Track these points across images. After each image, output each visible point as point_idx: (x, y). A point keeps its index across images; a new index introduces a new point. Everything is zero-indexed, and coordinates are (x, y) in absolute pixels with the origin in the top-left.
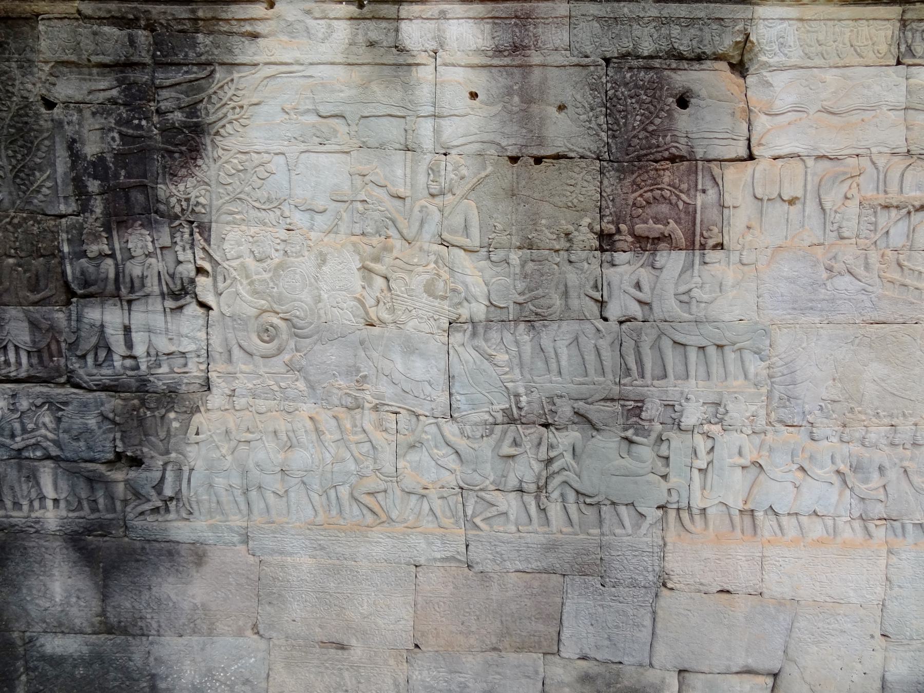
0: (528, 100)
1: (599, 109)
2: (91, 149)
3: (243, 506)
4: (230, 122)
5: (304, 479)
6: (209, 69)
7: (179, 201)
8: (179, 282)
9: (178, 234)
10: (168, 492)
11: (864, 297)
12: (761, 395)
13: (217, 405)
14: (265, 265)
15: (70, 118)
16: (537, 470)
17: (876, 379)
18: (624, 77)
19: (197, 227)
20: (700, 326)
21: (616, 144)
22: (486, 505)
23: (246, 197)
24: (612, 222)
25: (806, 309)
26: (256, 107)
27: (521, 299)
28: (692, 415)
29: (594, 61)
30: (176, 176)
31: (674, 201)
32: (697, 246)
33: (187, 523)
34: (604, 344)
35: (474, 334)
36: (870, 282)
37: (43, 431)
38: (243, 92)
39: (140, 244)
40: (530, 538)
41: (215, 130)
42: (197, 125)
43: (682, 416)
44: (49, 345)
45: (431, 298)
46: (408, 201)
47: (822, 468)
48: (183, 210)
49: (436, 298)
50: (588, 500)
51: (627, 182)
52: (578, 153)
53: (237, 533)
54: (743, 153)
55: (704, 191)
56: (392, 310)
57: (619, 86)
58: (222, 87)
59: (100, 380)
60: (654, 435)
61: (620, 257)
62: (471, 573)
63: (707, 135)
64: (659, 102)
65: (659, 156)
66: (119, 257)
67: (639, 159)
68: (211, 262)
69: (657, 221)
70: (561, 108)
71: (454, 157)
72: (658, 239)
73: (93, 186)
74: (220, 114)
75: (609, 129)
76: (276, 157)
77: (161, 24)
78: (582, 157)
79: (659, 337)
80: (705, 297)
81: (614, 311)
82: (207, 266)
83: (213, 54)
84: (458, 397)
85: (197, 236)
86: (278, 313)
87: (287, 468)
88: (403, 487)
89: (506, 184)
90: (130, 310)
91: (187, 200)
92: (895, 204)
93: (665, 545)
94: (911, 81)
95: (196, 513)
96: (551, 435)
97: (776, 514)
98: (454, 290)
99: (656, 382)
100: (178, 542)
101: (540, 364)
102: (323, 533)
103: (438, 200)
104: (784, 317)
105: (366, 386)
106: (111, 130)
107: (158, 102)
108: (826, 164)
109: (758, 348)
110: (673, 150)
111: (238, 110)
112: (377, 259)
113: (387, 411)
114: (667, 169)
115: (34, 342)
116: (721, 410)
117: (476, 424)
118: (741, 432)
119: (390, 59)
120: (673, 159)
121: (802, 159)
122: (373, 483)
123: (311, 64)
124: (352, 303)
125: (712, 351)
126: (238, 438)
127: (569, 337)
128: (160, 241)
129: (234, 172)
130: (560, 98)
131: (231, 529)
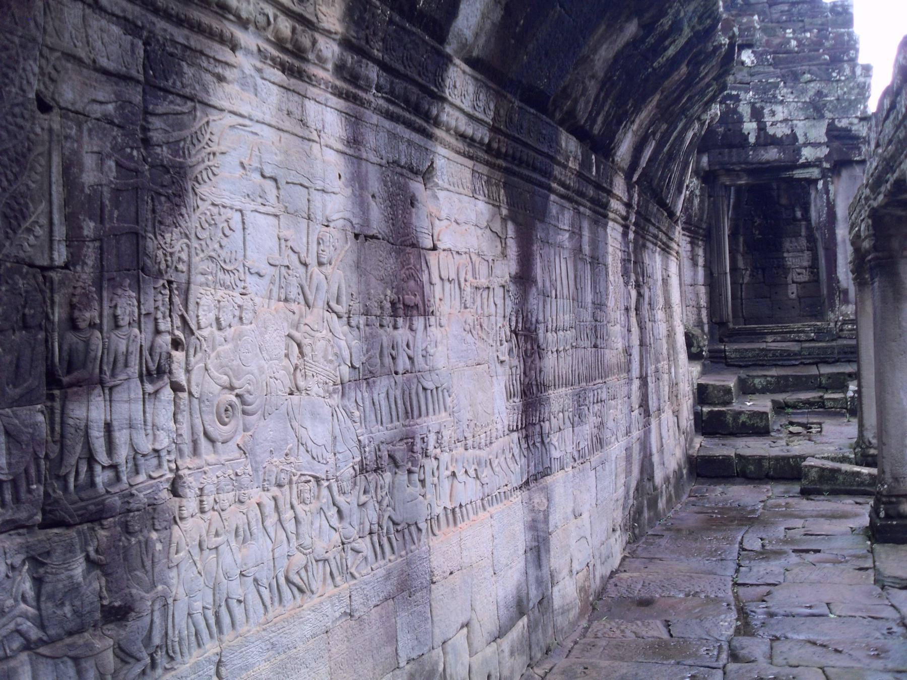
2: (89, 177)
3: (214, 629)
6: (190, 104)
10: (157, 640)
15: (68, 131)
33: (173, 673)
37: (23, 606)
39: (128, 309)
42: (181, 166)
44: (26, 471)
48: (167, 266)
59: (85, 508)
66: (105, 328)
73: (89, 228)
74: (199, 157)
77: (158, 41)
90: (111, 401)
106: (109, 156)
115: (9, 465)
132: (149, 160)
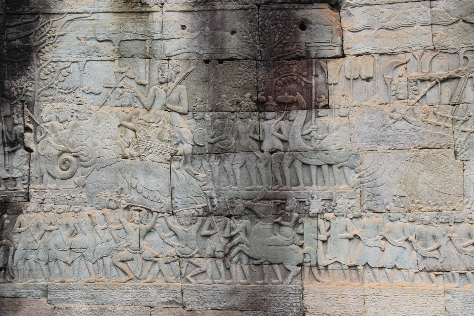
0: (214, 29)
1: (254, 32)
3: (46, 272)
4: (47, 45)
5: (84, 253)
6: (36, 16)
7: (17, 89)
8: (14, 136)
9: (15, 108)
11: (414, 133)
12: (356, 194)
13: (33, 209)
14: (65, 125)
16: (224, 244)
17: (426, 182)
18: (268, 14)
19: (26, 104)
20: (318, 154)
21: (265, 51)
22: (194, 267)
23: (55, 87)
24: (264, 95)
25: (380, 141)
26: (63, 37)
27: (212, 141)
28: (315, 208)
29: (251, 6)
30: (15, 75)
31: (299, 82)
32: (313, 107)
33: (10, 284)
34: (261, 165)
35: (185, 163)
36: (417, 124)
38: (55, 29)
40: (221, 287)
41: (38, 50)
42: (29, 47)
43: (309, 208)
45: (160, 142)
46: (147, 86)
47: (397, 238)
48: (18, 94)
49: (163, 141)
50: (255, 262)
51: (273, 71)
52: (243, 57)
53: (41, 289)
54: (338, 53)
55: (317, 76)
56: (137, 149)
57: (266, 19)
58: (43, 26)
60: (293, 220)
61: (270, 115)
62: (185, 311)
63: (317, 44)
64: (288, 28)
65: (289, 57)
67: (278, 59)
68: (33, 124)
69: (290, 93)
70: (233, 32)
71: (173, 61)
72: (291, 103)
74: (42, 41)
75: (260, 43)
76: (73, 64)
78: (245, 59)
79: (294, 160)
80: (320, 136)
81: (266, 146)
82: (31, 126)
83: (39, 8)
84: (177, 200)
85: (26, 109)
86: (71, 153)
87: (74, 247)
88: (143, 256)
89: (202, 75)
91: (21, 89)
92: (428, 78)
93: (303, 289)
94: (433, 9)
95: (16, 278)
96: (232, 222)
97: (371, 268)
98: (173, 137)
99: (293, 188)
100: (3, 297)
101: (224, 179)
102: (94, 287)
103: (164, 86)
104: (367, 147)
105: (122, 195)
107: (7, 34)
109: (352, 165)
110: (298, 53)
111: (52, 38)
112: (130, 120)
113: (134, 210)
114: (295, 64)
116: (333, 203)
117: (187, 216)
118: (346, 217)
119: (137, 9)
120: (299, 58)
121: (373, 56)
122: (126, 254)
123: (93, 13)
124: (115, 145)
125: (325, 168)
126: (45, 229)
127: (240, 162)
128: (4, 113)
129: (49, 72)
130: (232, 27)
131: (38, 287)
132: (6, 48)
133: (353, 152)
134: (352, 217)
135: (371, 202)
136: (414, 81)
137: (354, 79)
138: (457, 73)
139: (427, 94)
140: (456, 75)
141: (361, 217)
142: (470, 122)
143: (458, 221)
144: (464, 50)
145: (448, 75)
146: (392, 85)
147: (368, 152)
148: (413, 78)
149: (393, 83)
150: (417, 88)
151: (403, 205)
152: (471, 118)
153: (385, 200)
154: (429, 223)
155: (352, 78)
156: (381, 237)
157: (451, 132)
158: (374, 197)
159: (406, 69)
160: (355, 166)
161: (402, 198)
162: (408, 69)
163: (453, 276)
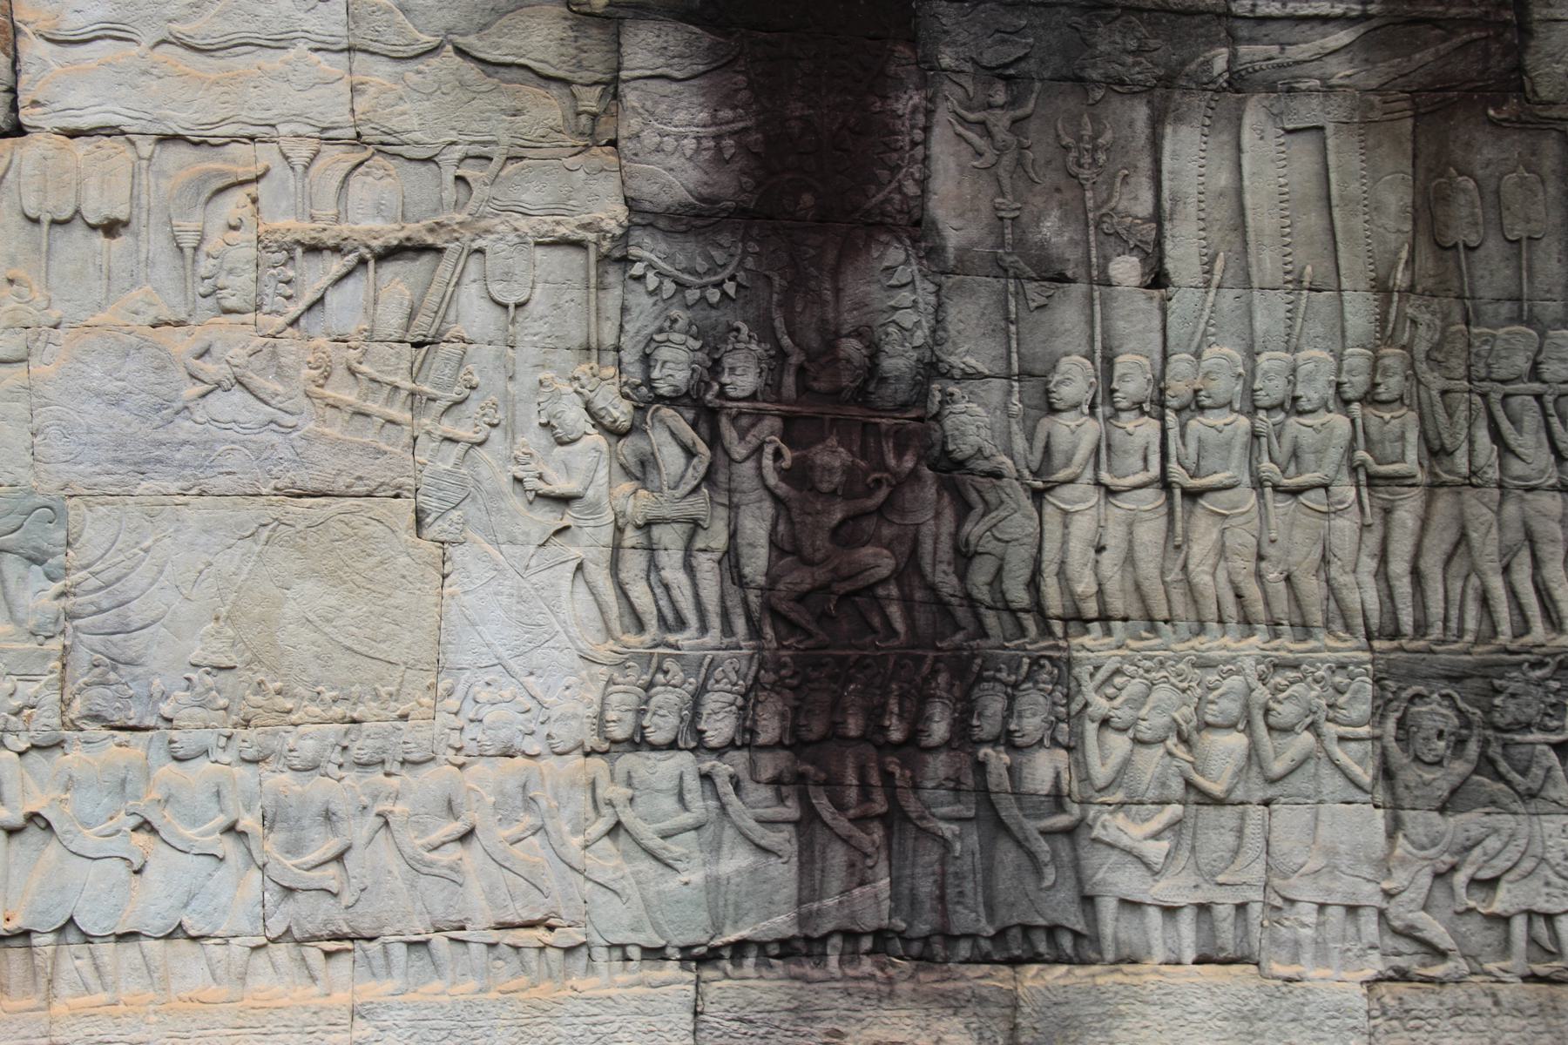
11: (276, 438)
12: (47, 657)
17: (312, 617)
25: (147, 461)
47: (194, 822)
92: (331, 242)
97: (87, 938)
108: (177, 155)
109: (36, 548)
121: (132, 143)
133: (40, 500)
134: (23, 746)
135: (101, 689)
136: (281, 249)
137: (55, 222)
138: (431, 230)
139: (328, 299)
140: (430, 240)
141: (59, 744)
142: (472, 407)
143: (415, 757)
144: (457, 152)
145: (402, 235)
146: (201, 256)
147: (101, 499)
148: (277, 236)
149: (205, 248)
150: (291, 274)
151: (222, 702)
152: (474, 395)
153: (157, 681)
154: (312, 767)
155: (46, 218)
156: (135, 821)
157: (407, 439)
158: (114, 669)
159: (255, 201)
160: (45, 553)
161: (222, 675)
162: (262, 202)
163: (386, 953)
